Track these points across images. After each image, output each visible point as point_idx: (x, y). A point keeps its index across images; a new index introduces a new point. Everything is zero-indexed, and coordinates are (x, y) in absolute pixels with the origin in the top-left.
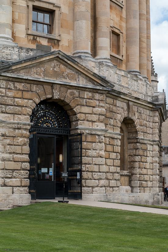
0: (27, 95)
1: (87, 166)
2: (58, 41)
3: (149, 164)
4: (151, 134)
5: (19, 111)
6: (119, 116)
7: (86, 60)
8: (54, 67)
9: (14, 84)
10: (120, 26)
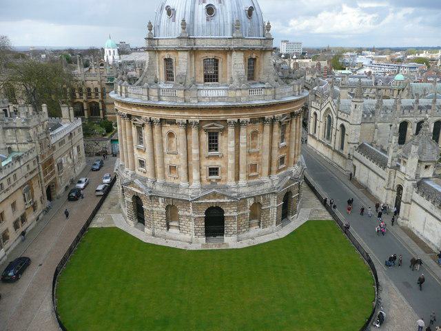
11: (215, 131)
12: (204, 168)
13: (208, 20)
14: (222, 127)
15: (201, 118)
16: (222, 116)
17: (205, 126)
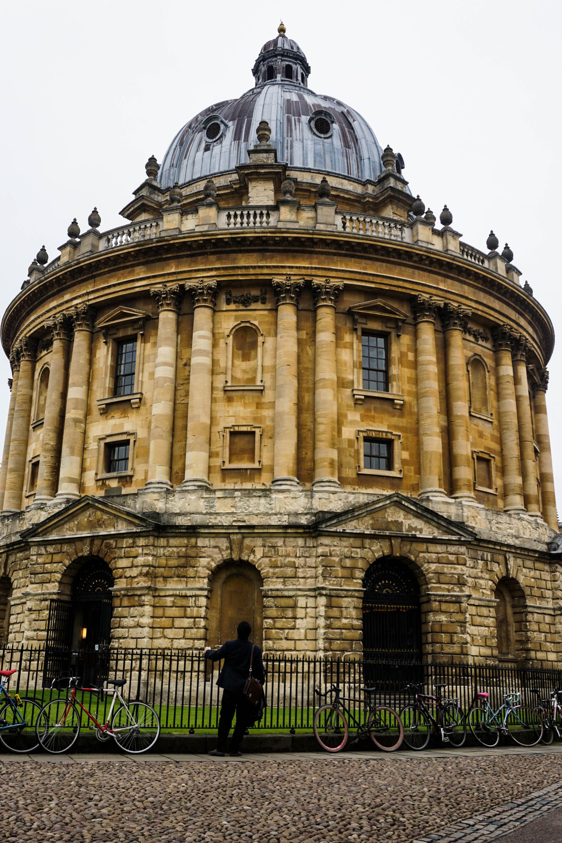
0: (57, 558)
1: (121, 641)
2: (131, 477)
3: (303, 631)
4: (311, 577)
5: (47, 578)
6: (204, 561)
7: (145, 494)
8: (90, 516)
9: (45, 548)
10: (255, 419)
11: (130, 332)
12: (93, 445)
13: (207, 149)
14: (138, 313)
15: (93, 299)
16: (139, 279)
17: (102, 322)
